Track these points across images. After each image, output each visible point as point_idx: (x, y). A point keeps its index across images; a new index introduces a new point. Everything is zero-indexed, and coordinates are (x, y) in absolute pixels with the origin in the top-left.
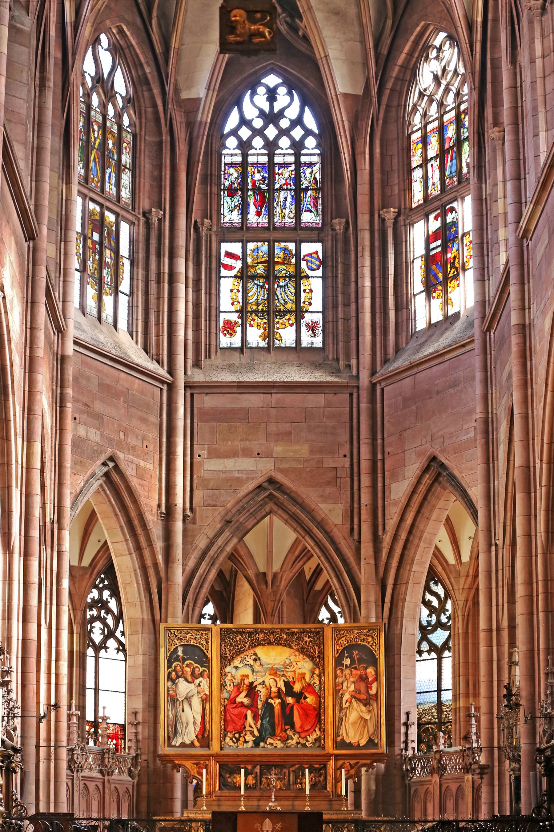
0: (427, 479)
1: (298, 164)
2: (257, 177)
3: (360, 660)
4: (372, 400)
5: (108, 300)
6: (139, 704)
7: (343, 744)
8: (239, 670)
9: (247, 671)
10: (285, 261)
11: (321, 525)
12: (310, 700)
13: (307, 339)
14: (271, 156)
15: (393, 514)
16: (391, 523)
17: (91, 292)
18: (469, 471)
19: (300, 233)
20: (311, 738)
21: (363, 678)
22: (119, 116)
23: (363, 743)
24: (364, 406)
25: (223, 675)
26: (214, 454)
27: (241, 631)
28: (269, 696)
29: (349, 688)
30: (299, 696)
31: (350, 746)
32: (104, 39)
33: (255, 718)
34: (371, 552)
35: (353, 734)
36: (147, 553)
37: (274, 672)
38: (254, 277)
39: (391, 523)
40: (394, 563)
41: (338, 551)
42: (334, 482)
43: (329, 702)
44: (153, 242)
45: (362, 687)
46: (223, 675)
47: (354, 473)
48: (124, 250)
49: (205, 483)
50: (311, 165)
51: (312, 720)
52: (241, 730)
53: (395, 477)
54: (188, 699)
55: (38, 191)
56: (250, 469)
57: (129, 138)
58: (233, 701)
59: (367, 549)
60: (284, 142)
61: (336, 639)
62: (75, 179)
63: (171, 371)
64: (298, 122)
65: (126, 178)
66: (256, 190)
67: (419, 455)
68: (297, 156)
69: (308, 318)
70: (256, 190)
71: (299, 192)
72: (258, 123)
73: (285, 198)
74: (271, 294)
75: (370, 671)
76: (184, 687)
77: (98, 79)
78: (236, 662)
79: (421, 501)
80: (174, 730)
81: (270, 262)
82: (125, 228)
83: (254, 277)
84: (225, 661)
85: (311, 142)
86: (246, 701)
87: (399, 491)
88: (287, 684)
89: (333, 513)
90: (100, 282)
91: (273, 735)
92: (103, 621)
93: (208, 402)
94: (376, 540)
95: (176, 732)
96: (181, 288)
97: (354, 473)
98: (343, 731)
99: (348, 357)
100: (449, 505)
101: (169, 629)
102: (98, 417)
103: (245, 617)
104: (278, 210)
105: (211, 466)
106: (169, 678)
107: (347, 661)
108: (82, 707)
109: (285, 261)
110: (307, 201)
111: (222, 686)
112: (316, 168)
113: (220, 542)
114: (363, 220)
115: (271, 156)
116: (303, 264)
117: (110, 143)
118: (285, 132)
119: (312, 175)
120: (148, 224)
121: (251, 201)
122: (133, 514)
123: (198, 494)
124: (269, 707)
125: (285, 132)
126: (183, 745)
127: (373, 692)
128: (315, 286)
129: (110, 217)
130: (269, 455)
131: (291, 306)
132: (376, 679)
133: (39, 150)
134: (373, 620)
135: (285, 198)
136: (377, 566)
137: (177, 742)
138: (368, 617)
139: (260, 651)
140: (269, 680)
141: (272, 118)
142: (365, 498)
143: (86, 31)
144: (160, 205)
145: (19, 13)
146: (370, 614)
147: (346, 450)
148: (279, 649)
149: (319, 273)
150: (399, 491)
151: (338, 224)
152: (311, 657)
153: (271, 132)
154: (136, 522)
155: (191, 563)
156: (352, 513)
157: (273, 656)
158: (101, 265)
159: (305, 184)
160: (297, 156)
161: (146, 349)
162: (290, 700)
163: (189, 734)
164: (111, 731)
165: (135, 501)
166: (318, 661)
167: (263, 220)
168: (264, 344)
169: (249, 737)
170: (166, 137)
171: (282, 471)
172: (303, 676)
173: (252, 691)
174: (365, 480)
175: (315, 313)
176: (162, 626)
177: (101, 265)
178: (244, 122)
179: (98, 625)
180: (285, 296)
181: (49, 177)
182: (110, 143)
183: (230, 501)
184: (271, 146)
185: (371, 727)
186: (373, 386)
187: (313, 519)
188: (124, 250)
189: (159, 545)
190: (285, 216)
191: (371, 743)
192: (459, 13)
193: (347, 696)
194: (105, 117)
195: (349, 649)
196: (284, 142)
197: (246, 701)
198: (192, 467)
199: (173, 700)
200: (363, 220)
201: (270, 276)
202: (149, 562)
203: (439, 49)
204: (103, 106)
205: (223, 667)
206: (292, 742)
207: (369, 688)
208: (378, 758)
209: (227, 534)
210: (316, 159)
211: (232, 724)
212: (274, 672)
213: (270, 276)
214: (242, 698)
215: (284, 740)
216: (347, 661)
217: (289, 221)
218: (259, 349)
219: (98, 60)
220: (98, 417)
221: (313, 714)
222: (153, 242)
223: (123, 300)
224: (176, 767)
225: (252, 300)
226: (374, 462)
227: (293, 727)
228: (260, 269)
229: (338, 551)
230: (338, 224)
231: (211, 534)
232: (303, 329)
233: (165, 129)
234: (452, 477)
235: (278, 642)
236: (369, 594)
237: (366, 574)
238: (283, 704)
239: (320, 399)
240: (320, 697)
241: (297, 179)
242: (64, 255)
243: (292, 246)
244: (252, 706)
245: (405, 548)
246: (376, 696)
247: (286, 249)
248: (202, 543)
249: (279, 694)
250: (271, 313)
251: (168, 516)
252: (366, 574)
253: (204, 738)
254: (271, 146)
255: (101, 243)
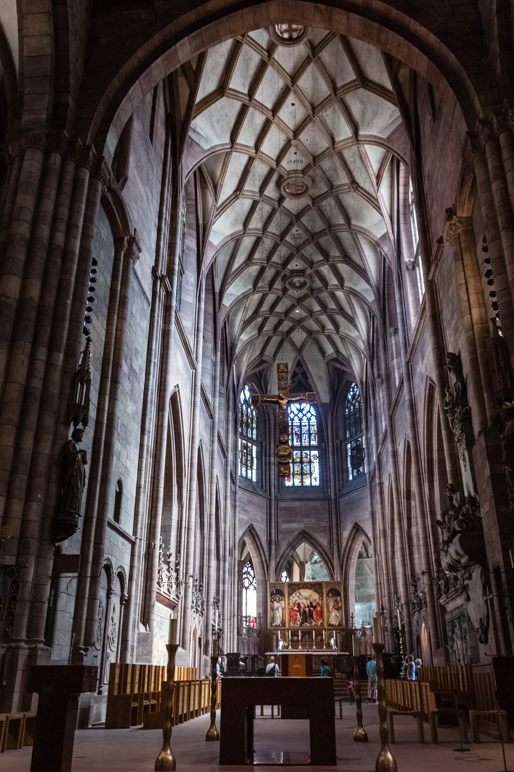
0: (354, 530)
1: (309, 425)
2: (297, 430)
3: (335, 595)
4: (336, 504)
5: (249, 472)
6: (261, 611)
7: (330, 625)
8: (295, 598)
9: (297, 598)
10: (306, 457)
11: (321, 546)
12: (319, 608)
13: (314, 484)
14: (301, 423)
15: (344, 542)
16: (344, 545)
17: (244, 469)
18: (368, 528)
19: (310, 448)
20: (319, 623)
21: (336, 601)
22: (252, 412)
23: (337, 624)
24: (333, 505)
25: (289, 600)
26: (285, 522)
27: (295, 584)
28: (305, 607)
29: (332, 604)
30: (315, 607)
31: (333, 625)
32: (247, 387)
33: (300, 615)
34: (337, 555)
35: (334, 621)
36: (263, 557)
37: (306, 598)
38: (296, 463)
39: (344, 545)
40: (345, 559)
41: (326, 555)
42: (324, 531)
43: (325, 609)
44: (264, 452)
45: (336, 604)
46: (289, 600)
47: (331, 528)
48: (254, 455)
49: (282, 532)
50: (313, 426)
51: (319, 616)
52: (296, 620)
53: (344, 529)
54: (277, 609)
55: (227, 442)
56: (296, 526)
57: (255, 418)
58: (293, 609)
59: (336, 555)
60: (305, 418)
61: (326, 587)
62: (238, 434)
63: (270, 495)
64: (309, 412)
65: (255, 432)
66: (296, 434)
67: (352, 522)
68: (309, 423)
69: (314, 476)
70: (296, 434)
71: (310, 434)
72: (296, 412)
73: (305, 437)
74: (302, 468)
75: (338, 598)
76: (276, 604)
77: (245, 401)
78: (293, 595)
79: (353, 538)
80: (273, 620)
81: (301, 458)
82: (254, 448)
83: (296, 463)
84: (290, 595)
85: (313, 419)
86: (297, 609)
87: (346, 534)
88: (311, 603)
89: (324, 541)
90: (247, 466)
91: (306, 621)
92: (248, 579)
93: (282, 504)
94: (339, 551)
95: (274, 621)
96: (272, 467)
97: (331, 528)
98: (330, 620)
99: (327, 489)
100: (362, 539)
101: (270, 584)
102: (246, 511)
103: (296, 579)
104: (303, 441)
105: (284, 526)
106: (271, 601)
107: (330, 595)
108: (241, 612)
109: (306, 457)
110: (312, 438)
111: (289, 604)
112: (315, 426)
113: (287, 552)
114: (330, 444)
115: (301, 423)
116: (312, 458)
117: (249, 421)
118: (304, 415)
119: (314, 429)
120: (262, 446)
121: (295, 437)
122: (258, 543)
123: (280, 536)
124: (305, 611)
125: (304, 415)
126: (276, 626)
127: (340, 605)
128: (316, 466)
129: (250, 445)
130: (303, 522)
131: (308, 472)
132: (341, 601)
133: (227, 430)
134: (339, 580)
135: (305, 437)
136: (339, 560)
137: (274, 625)
138: (337, 578)
139: (301, 591)
140: (305, 601)
141: (301, 411)
142: (335, 537)
143: (241, 386)
144: (265, 440)
145: (222, 387)
146: (338, 578)
147: (328, 520)
148: (307, 590)
149: (317, 460)
150: (346, 534)
151: (323, 445)
152: (318, 593)
153: (300, 415)
154: (259, 546)
155: (278, 560)
156: (331, 542)
157: (306, 593)
158: (247, 460)
159: (312, 432)
160: (309, 423)
161: (262, 487)
162: (312, 609)
163: (278, 622)
164: (251, 620)
165: (259, 539)
166: (321, 595)
167: (299, 444)
168: (300, 485)
169: (298, 623)
170: (267, 418)
171: (308, 528)
172: (316, 600)
173: (299, 605)
174: (334, 530)
175: (316, 473)
176: (268, 583)
177: (247, 460)
178: (292, 412)
179: (247, 580)
180: (306, 468)
181: (231, 435)
182: (249, 421)
183: (291, 538)
184: (301, 420)
185: (340, 618)
186: (336, 499)
187: (318, 544)
188: (254, 455)
189: (267, 554)
190: (305, 443)
191: (340, 624)
192: (358, 379)
193: (331, 607)
194: (247, 412)
195: (331, 590)
196: (305, 418)
197: (297, 609)
198: (277, 527)
199: (272, 609)
200: (330, 444)
201: (301, 462)
202: (264, 560)
203: (353, 388)
204: (247, 409)
205: (289, 597)
206: (313, 624)
207: (338, 604)
208: (343, 630)
209: (289, 549)
210: (315, 424)
211: (292, 618)
212: (306, 598)
213: (301, 462)
214: (296, 608)
215: (310, 623)
216: (330, 595)
217: (307, 444)
218: (298, 486)
219: (245, 394)
220: (246, 511)
221: (320, 614)
222: (264, 452)
223: (254, 472)
224: (274, 634)
225: (296, 470)
226: (337, 524)
227: (313, 619)
228: (298, 460)
229: (326, 555)
230: (323, 445)
231: (284, 549)
232: (312, 479)
233: (267, 415)
234: (363, 530)
235: (307, 588)
236: (337, 570)
237: (336, 562)
238: (310, 610)
239: (318, 503)
240: (322, 608)
241: (309, 431)
242: (236, 459)
243: (308, 452)
244: (299, 611)
245: (348, 554)
246: (341, 607)
247: (306, 453)
248: (281, 553)
249: (308, 607)
250: (302, 474)
251: (270, 544)
252: (336, 562)
253: (283, 623)
254: (301, 420)
255: (247, 453)
